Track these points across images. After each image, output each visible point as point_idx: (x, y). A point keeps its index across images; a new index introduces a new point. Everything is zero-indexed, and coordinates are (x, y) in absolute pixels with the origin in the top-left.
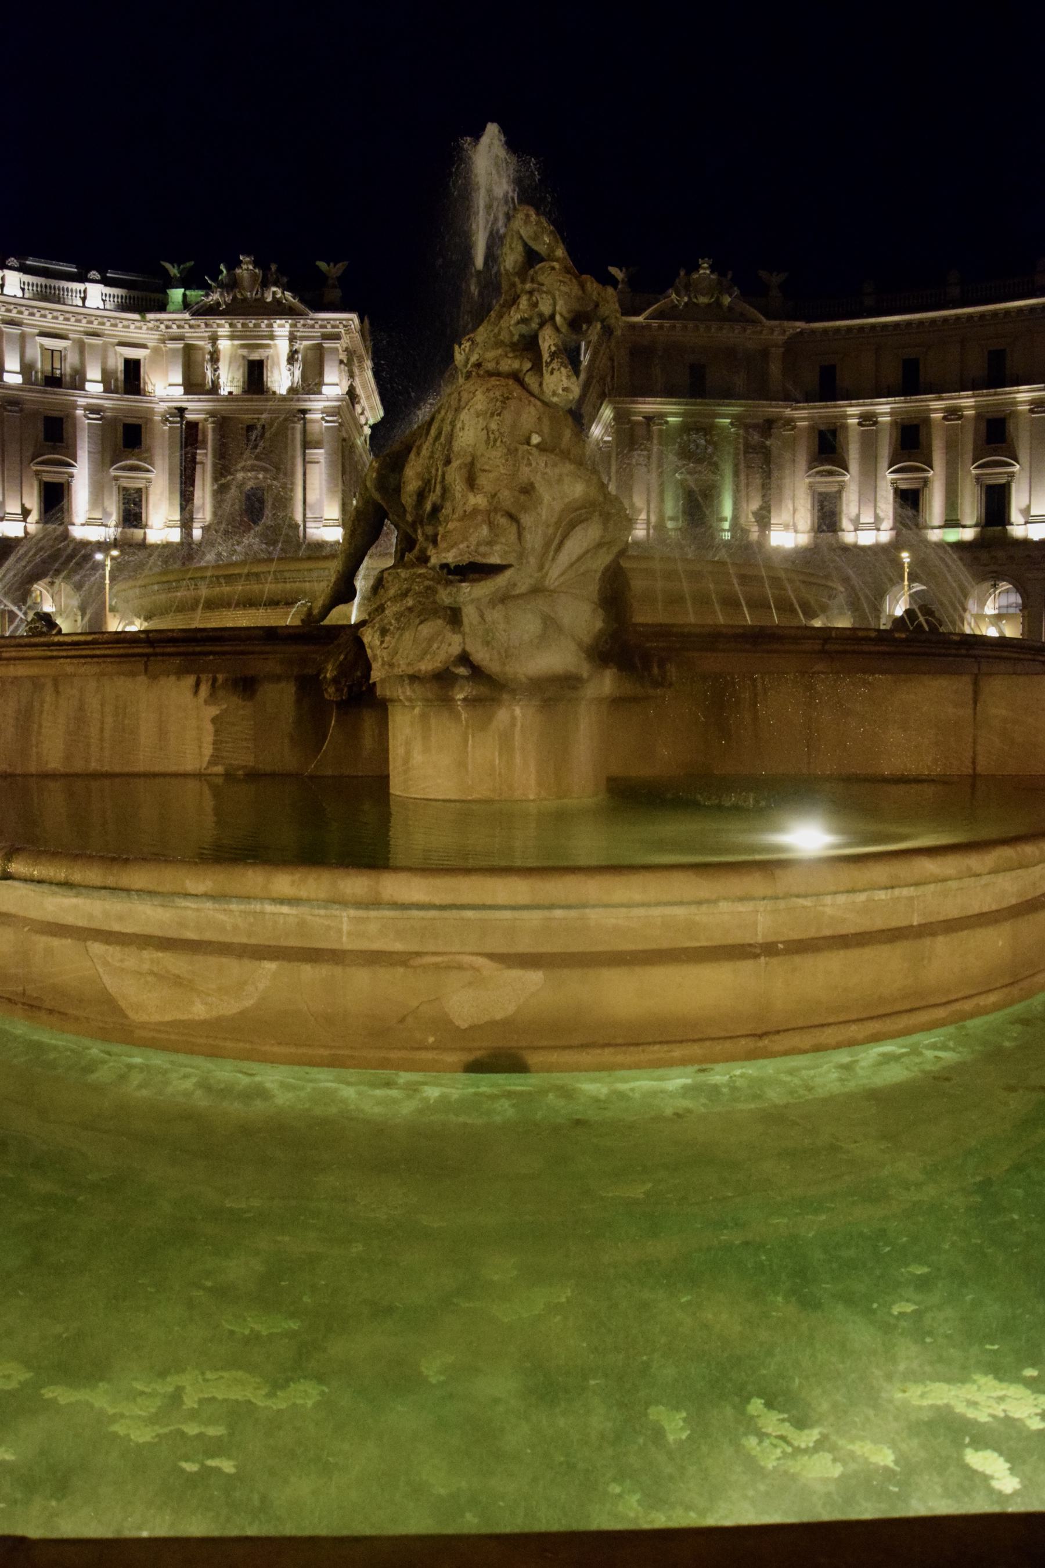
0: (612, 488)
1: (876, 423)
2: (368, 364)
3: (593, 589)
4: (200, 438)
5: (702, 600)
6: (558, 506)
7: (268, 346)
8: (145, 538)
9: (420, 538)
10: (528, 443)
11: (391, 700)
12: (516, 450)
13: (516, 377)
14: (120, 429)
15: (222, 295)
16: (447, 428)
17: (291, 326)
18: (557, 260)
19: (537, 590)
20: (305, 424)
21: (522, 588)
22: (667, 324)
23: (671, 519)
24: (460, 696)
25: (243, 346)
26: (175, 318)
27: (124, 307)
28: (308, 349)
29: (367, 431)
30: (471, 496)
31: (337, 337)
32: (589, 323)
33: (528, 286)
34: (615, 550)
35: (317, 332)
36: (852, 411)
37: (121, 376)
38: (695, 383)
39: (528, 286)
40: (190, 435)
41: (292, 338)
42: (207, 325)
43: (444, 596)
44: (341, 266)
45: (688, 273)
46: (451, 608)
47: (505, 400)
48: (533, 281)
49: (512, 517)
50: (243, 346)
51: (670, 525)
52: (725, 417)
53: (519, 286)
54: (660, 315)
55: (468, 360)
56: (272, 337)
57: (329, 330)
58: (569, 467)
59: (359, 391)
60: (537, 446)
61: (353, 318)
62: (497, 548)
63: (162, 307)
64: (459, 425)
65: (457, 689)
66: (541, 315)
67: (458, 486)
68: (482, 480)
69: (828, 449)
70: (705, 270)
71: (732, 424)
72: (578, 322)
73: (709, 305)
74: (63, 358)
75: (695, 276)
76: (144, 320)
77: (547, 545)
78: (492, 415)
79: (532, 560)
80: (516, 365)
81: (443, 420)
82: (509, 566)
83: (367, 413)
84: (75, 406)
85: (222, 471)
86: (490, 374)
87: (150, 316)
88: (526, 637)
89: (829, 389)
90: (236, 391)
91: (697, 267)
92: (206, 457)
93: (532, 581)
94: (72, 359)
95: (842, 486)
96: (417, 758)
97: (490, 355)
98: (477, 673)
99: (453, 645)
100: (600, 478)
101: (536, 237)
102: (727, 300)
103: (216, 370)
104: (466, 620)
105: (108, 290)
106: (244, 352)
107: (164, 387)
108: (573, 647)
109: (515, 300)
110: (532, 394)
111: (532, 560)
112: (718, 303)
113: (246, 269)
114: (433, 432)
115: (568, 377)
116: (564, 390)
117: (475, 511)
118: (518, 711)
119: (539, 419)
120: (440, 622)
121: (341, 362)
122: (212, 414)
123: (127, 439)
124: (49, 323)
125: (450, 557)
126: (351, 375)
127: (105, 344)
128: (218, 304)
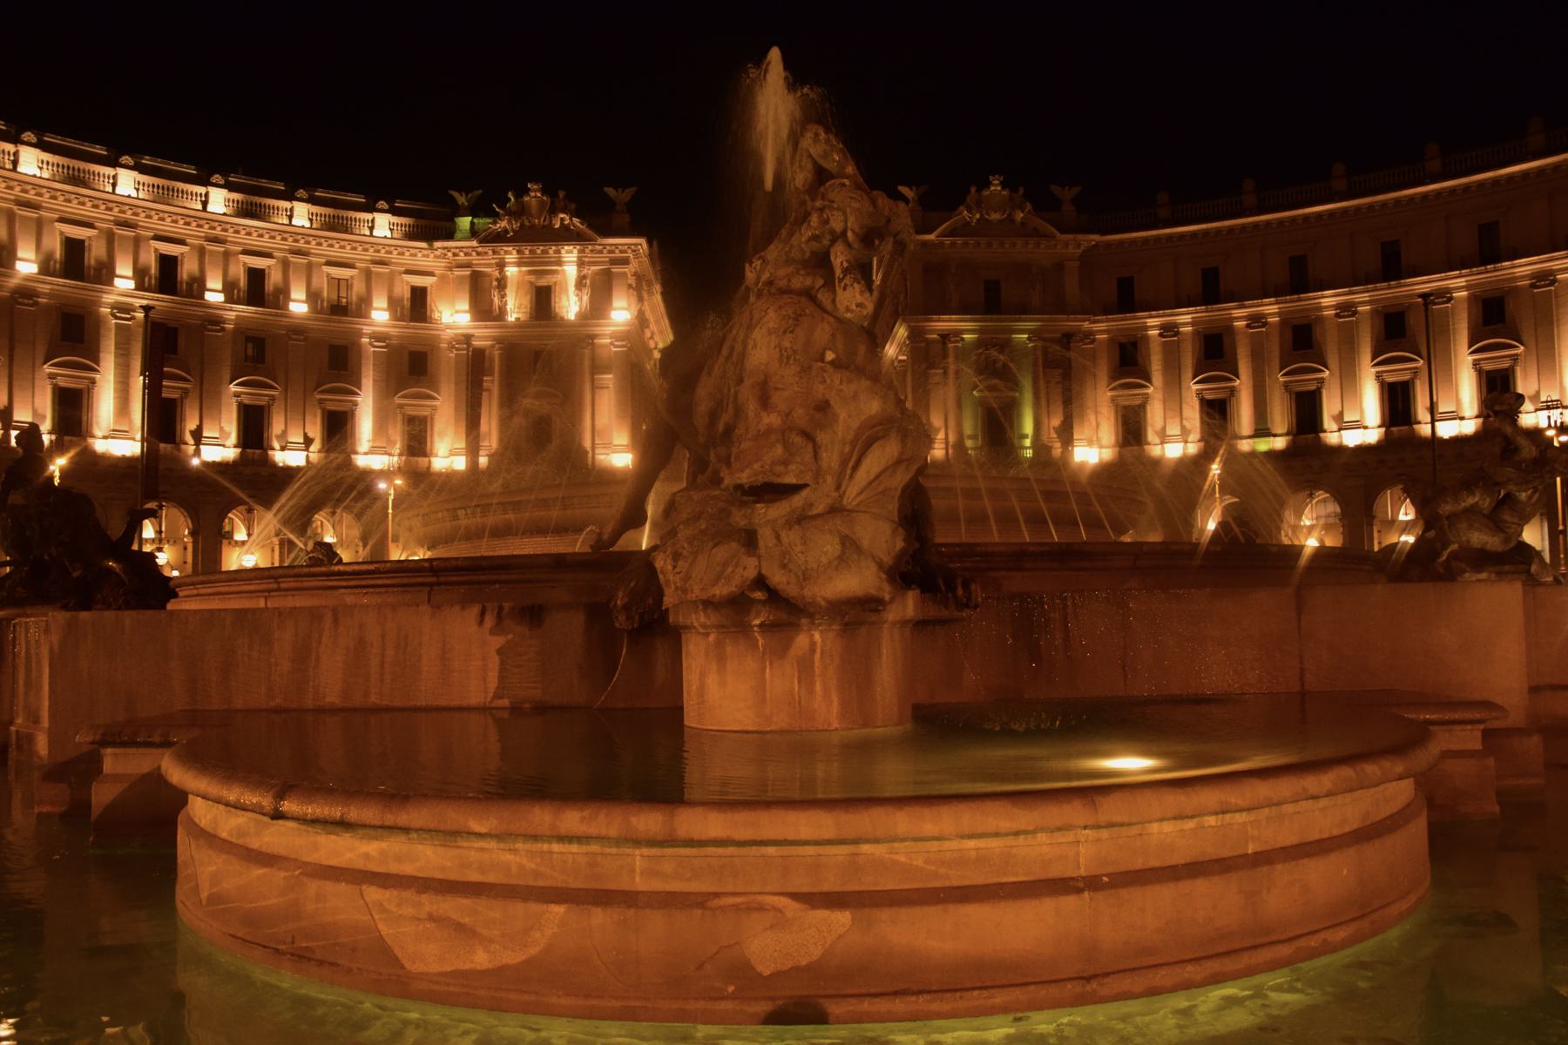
0: (909, 405)
1: (1177, 334)
2: (658, 288)
3: (893, 507)
4: (487, 365)
5: (1007, 519)
6: (855, 424)
7: (556, 272)
8: (429, 467)
9: (712, 458)
10: (822, 359)
11: (685, 627)
12: (810, 368)
13: (809, 294)
14: (406, 357)
15: (509, 222)
16: (739, 347)
17: (580, 252)
18: (847, 177)
19: (835, 510)
20: (593, 351)
21: (820, 508)
22: (959, 241)
23: (973, 437)
24: (757, 622)
25: (530, 273)
26: (461, 247)
27: (411, 235)
28: (597, 273)
29: (657, 355)
30: (764, 414)
31: (625, 262)
32: (881, 237)
33: (818, 204)
34: (915, 467)
35: (605, 257)
37: (407, 304)
38: (991, 300)
39: (818, 204)
40: (475, 364)
41: (581, 264)
42: (494, 252)
43: (739, 518)
44: (630, 191)
45: (979, 190)
46: (746, 531)
47: (797, 318)
48: (823, 198)
49: (808, 436)
50: (530, 273)
51: (969, 443)
53: (809, 203)
54: (952, 233)
55: (759, 278)
56: (560, 263)
57: (618, 254)
58: (866, 383)
59: (648, 314)
60: (832, 363)
61: (641, 243)
62: (792, 467)
63: (450, 235)
64: (751, 343)
65: (753, 614)
66: (832, 232)
67: (752, 407)
68: (778, 399)
69: (1129, 361)
70: (996, 187)
72: (869, 238)
73: (1001, 221)
74: (349, 286)
75: (986, 193)
76: (431, 248)
77: (844, 464)
78: (785, 332)
79: (829, 479)
80: (809, 282)
81: (734, 339)
82: (806, 485)
83: (657, 338)
84: (360, 334)
85: (509, 400)
86: (782, 292)
87: (437, 244)
88: (824, 560)
89: (1127, 300)
90: (523, 317)
91: (988, 184)
92: (493, 384)
93: (829, 501)
94: (359, 287)
95: (1146, 398)
96: (712, 681)
97: (782, 272)
98: (775, 597)
99: (749, 568)
100: (896, 394)
101: (825, 156)
103: (503, 296)
104: (761, 543)
105: (395, 219)
106: (532, 278)
107: (453, 316)
108: (874, 568)
109: (805, 217)
110: (825, 311)
111: (829, 479)
112: (1011, 219)
113: (535, 196)
114: (725, 351)
115: (861, 293)
116: (858, 305)
117: (770, 430)
118: (817, 636)
119: (833, 335)
120: (734, 545)
121: (630, 286)
122: (499, 340)
123: (412, 366)
124: (336, 252)
125: (744, 478)
126: (640, 299)
127: (392, 273)
128: (506, 231)
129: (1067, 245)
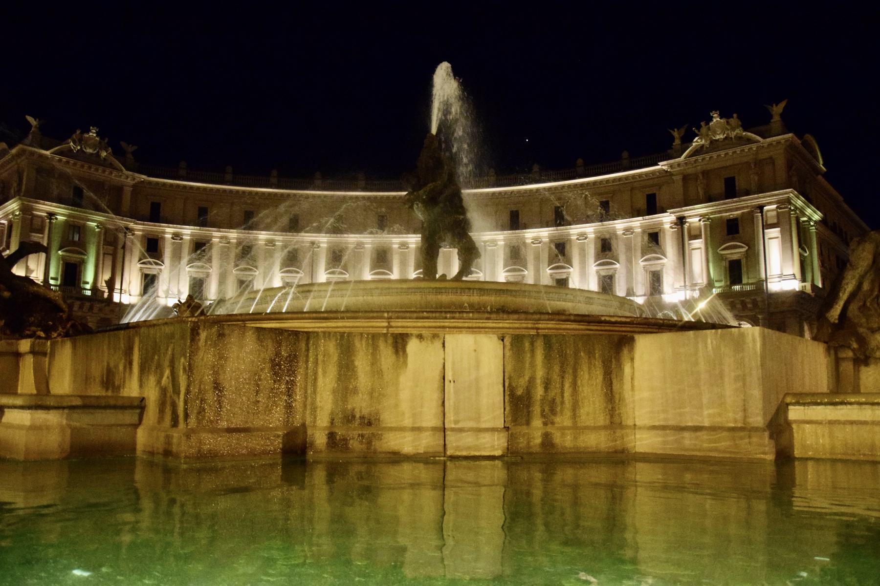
36: (169, 231)
52: (94, 222)
71: (98, 226)
91: (88, 131)
102: (104, 154)
112: (98, 155)
129: (127, 177)
